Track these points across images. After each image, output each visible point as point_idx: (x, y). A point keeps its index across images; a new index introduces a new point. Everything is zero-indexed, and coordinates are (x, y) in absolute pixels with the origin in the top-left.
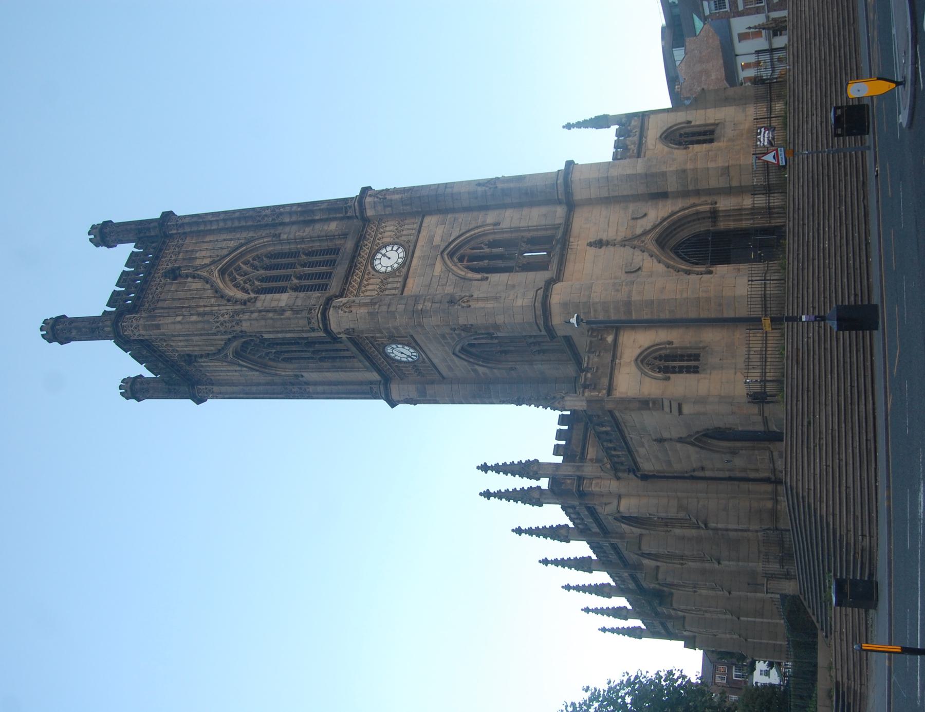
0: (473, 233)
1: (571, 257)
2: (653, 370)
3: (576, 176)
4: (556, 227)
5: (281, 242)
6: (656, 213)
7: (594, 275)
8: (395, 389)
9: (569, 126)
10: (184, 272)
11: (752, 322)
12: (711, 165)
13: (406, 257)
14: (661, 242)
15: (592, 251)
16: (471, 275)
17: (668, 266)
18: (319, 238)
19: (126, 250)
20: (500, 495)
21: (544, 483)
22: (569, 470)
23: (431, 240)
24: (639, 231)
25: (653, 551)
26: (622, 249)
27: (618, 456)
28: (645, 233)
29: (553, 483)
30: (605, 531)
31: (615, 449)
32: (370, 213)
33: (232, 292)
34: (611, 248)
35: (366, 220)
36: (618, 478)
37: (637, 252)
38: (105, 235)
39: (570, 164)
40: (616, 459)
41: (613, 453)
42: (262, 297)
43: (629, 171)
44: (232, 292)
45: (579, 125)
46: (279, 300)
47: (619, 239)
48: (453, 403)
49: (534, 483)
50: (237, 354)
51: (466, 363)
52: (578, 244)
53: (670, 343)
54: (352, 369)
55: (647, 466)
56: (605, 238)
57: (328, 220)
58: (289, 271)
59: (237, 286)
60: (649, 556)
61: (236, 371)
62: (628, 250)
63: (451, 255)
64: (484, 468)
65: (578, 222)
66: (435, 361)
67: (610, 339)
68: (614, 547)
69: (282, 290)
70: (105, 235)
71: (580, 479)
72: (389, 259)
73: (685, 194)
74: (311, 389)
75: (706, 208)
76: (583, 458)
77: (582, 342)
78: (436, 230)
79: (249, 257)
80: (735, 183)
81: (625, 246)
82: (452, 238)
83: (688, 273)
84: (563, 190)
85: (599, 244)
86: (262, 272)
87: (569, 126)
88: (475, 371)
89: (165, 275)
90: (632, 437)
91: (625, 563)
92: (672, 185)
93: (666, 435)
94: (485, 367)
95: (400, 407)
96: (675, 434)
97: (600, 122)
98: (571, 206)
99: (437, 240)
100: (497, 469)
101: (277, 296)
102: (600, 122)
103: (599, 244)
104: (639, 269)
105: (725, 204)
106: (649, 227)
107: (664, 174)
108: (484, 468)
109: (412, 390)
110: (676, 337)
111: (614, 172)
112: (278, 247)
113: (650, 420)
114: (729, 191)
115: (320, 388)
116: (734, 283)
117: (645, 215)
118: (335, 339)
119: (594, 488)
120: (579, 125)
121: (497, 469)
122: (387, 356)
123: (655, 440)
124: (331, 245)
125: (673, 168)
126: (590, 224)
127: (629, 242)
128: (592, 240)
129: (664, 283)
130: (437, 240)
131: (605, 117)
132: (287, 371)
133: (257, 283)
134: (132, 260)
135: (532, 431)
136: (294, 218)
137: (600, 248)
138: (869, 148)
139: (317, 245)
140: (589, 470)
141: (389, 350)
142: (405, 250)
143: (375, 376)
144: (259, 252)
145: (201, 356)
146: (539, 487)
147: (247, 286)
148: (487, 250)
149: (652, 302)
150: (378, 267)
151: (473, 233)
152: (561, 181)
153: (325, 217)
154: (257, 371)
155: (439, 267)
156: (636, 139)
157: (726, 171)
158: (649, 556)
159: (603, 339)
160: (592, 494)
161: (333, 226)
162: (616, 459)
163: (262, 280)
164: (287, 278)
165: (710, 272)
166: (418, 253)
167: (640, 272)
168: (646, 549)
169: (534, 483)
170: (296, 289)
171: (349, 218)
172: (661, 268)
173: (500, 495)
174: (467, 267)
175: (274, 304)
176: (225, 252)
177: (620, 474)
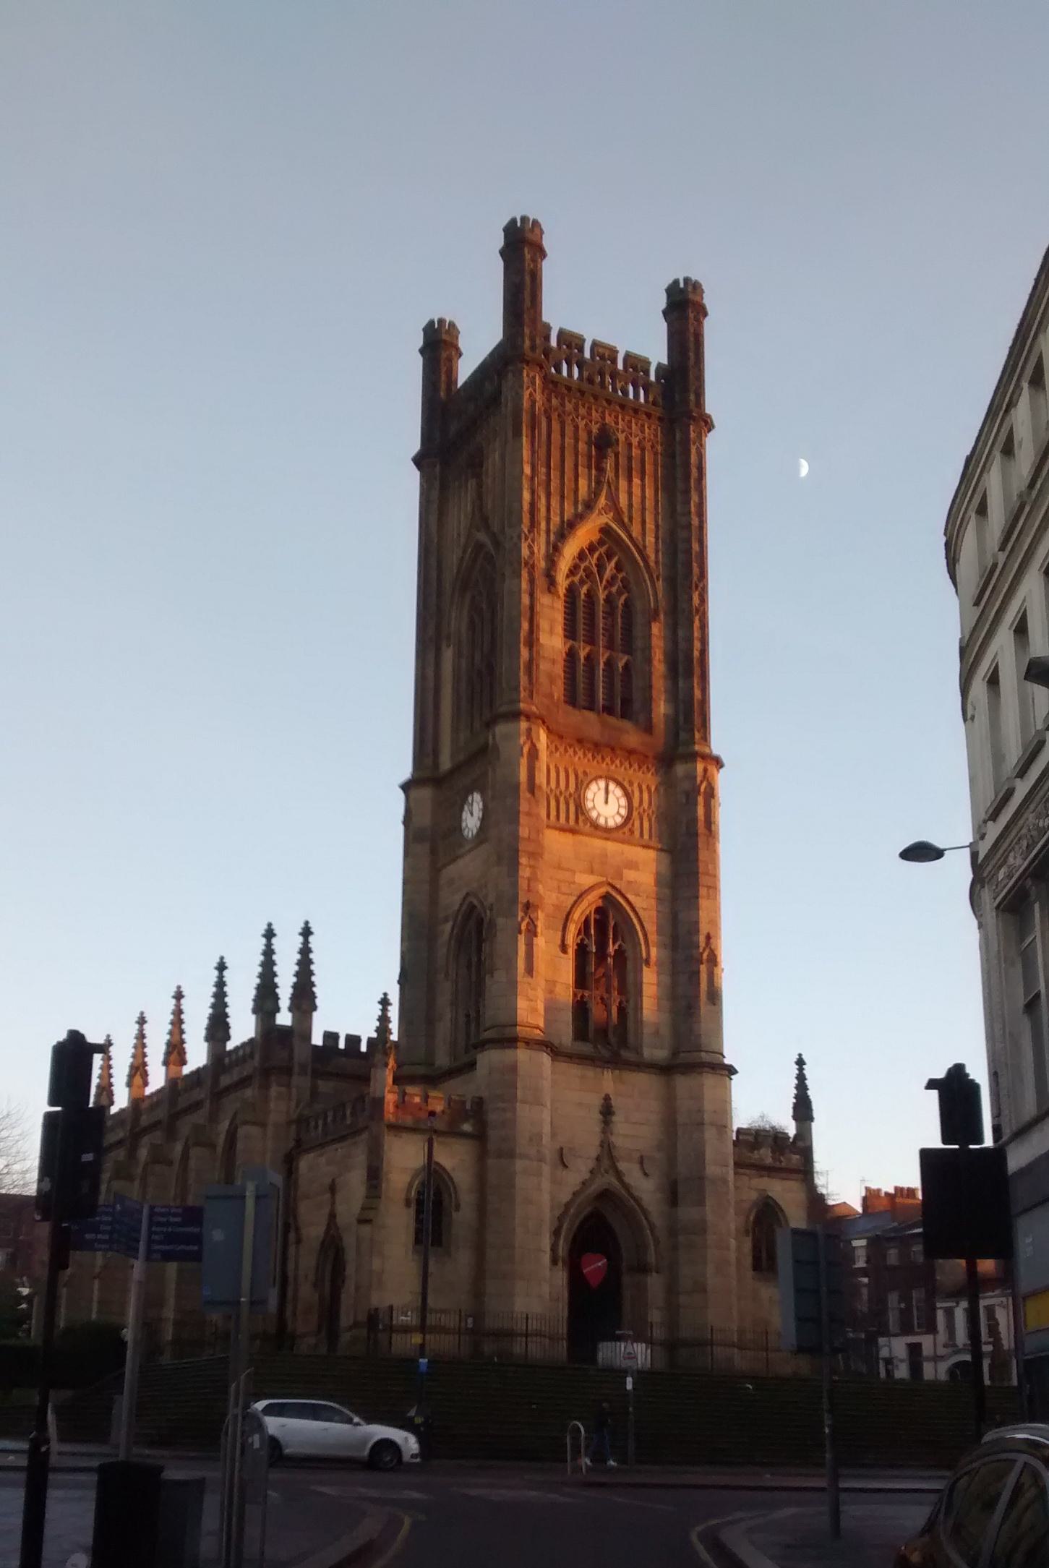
0: (638, 927)
1: (590, 1072)
2: (422, 1184)
3: (709, 1080)
4: (638, 1051)
6: (646, 1189)
7: (557, 1106)
8: (425, 793)
9: (800, 1062)
10: (609, 465)
11: (478, 1315)
12: (710, 1270)
13: (607, 830)
14: (605, 1195)
15: (597, 1101)
16: (572, 929)
17: (568, 1206)
19: (653, 347)
22: (300, 1055)
23: (633, 865)
24: (622, 1166)
25: (192, 1163)
26: (598, 1143)
27: (316, 1127)
28: (619, 1175)
29: (284, 1031)
30: (218, 1095)
31: (325, 1124)
33: (570, 550)
34: (597, 1128)
36: (289, 1123)
37: (591, 1164)
38: (684, 307)
39: (731, 1071)
40: (313, 1124)
41: (320, 1123)
42: (560, 605)
43: (709, 1155)
44: (570, 550)
45: (801, 1078)
46: (551, 632)
47: (613, 1139)
48: (405, 882)
50: (479, 546)
51: (456, 907)
52: (608, 1081)
53: (458, 1208)
54: (455, 730)
55: (304, 1163)
56: (614, 1118)
58: (601, 641)
59: (581, 556)
60: (185, 1156)
61: (459, 535)
62: (594, 1151)
63: (606, 897)
65: (643, 1082)
67: (467, 1127)
68: (197, 1105)
69: (570, 633)
70: (684, 307)
71: (288, 1071)
72: (606, 804)
73: (673, 1232)
74: (431, 657)
75: (652, 1258)
76: (316, 1074)
77: (462, 1088)
78: (641, 872)
80: (683, 1299)
81: (601, 1146)
82: (629, 896)
83: (556, 1233)
84: (694, 1059)
85: (607, 1111)
86: (602, 596)
87: (800, 1062)
88: (446, 920)
89: (604, 430)
90: (338, 1150)
91: (175, 1116)
92: (686, 1213)
94: (452, 937)
95: (401, 795)
96: (340, 1209)
97: (803, 1109)
98: (666, 1070)
99: (630, 875)
101: (559, 629)
102: (803, 1109)
103: (607, 1111)
104: (565, 1166)
105: (655, 1283)
106: (626, 1179)
107: (701, 1202)
109: (425, 820)
110: (463, 1217)
111: (710, 1134)
113: (356, 1181)
114: (672, 1290)
115: (430, 673)
116: (536, 1293)
117: (646, 1174)
118: (489, 724)
119: (274, 1090)
120: (801, 1078)
122: (470, 791)
123: (333, 1181)
124: (637, 706)
125: (710, 1217)
126: (638, 1100)
127: (607, 1154)
128: (613, 1102)
129: (542, 1198)
130: (630, 875)
131: (810, 1118)
132: (457, 621)
133: (584, 590)
134: (636, 364)
135: (357, 996)
137: (601, 1113)
139: (637, 682)
140: (301, 1082)
141: (477, 797)
142: (618, 828)
143: (446, 763)
145: (480, 486)
147: (581, 573)
148: (611, 949)
149: (513, 1186)
150: (593, 787)
151: (638, 927)
152: (705, 1057)
153: (681, 697)
154: (458, 572)
155: (586, 880)
156: (769, 1161)
157: (701, 1288)
158: (185, 1156)
159: (466, 1120)
160: (265, 1087)
162: (313, 1124)
163: (590, 595)
164: (591, 640)
165: (554, 1261)
166: (611, 847)
167: (561, 1167)
168: (195, 1152)
170: (571, 655)
172: (565, 1197)
174: (587, 922)
175: (544, 624)
176: (636, 531)
177: (294, 1127)
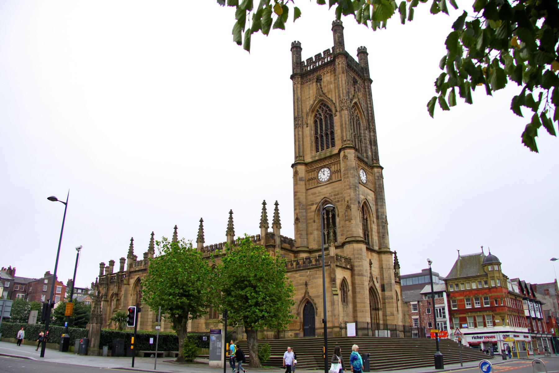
5: (364, 130)
18: (366, 147)
20: (264, 209)
21: (270, 230)
29: (271, 233)
32: (376, 170)
35: (372, 167)
49: (270, 225)
57: (372, 151)
64: (277, 204)
66: (319, 188)
79: (359, 115)
93: (309, 287)
100: (276, 209)
108: (277, 204)
112: (362, 128)
121: (276, 209)
136: (372, 137)
138: (462, 366)
144: (361, 120)
146: (268, 227)
161: (370, 153)
169: (270, 225)
171: (373, 160)
173: (264, 209)
